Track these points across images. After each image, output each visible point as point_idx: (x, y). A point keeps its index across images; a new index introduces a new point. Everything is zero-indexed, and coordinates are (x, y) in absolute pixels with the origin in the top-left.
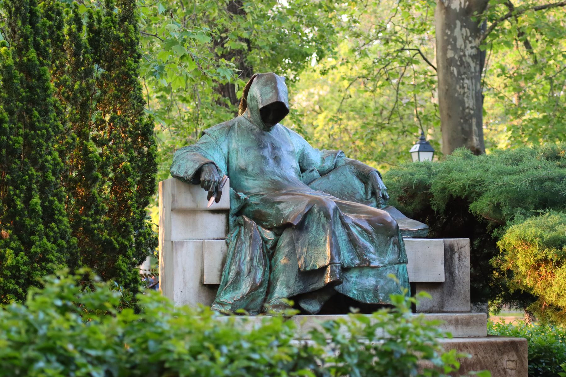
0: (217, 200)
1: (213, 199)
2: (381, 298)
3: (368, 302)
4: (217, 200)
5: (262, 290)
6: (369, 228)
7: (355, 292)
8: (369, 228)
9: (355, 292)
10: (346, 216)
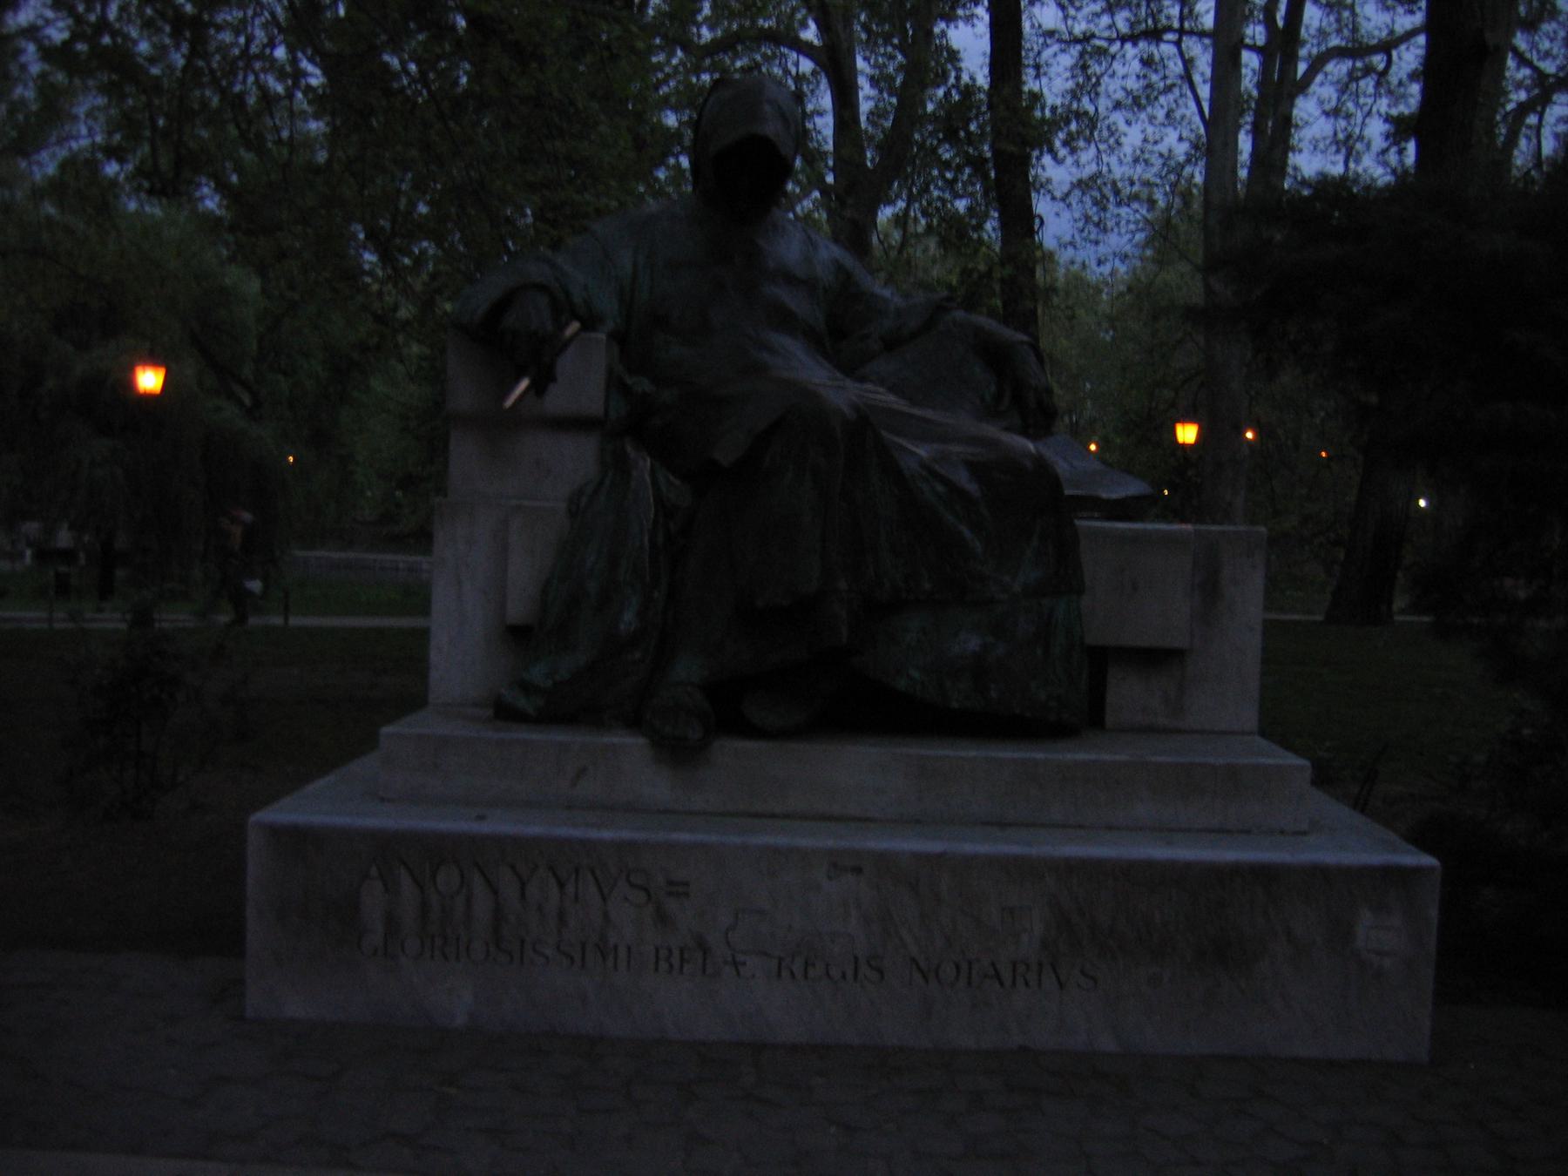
0: (538, 388)
1: (524, 384)
2: (993, 694)
3: (955, 705)
4: (538, 388)
5: (638, 655)
6: (972, 488)
7: (916, 674)
8: (972, 488)
9: (916, 674)
10: (905, 449)
